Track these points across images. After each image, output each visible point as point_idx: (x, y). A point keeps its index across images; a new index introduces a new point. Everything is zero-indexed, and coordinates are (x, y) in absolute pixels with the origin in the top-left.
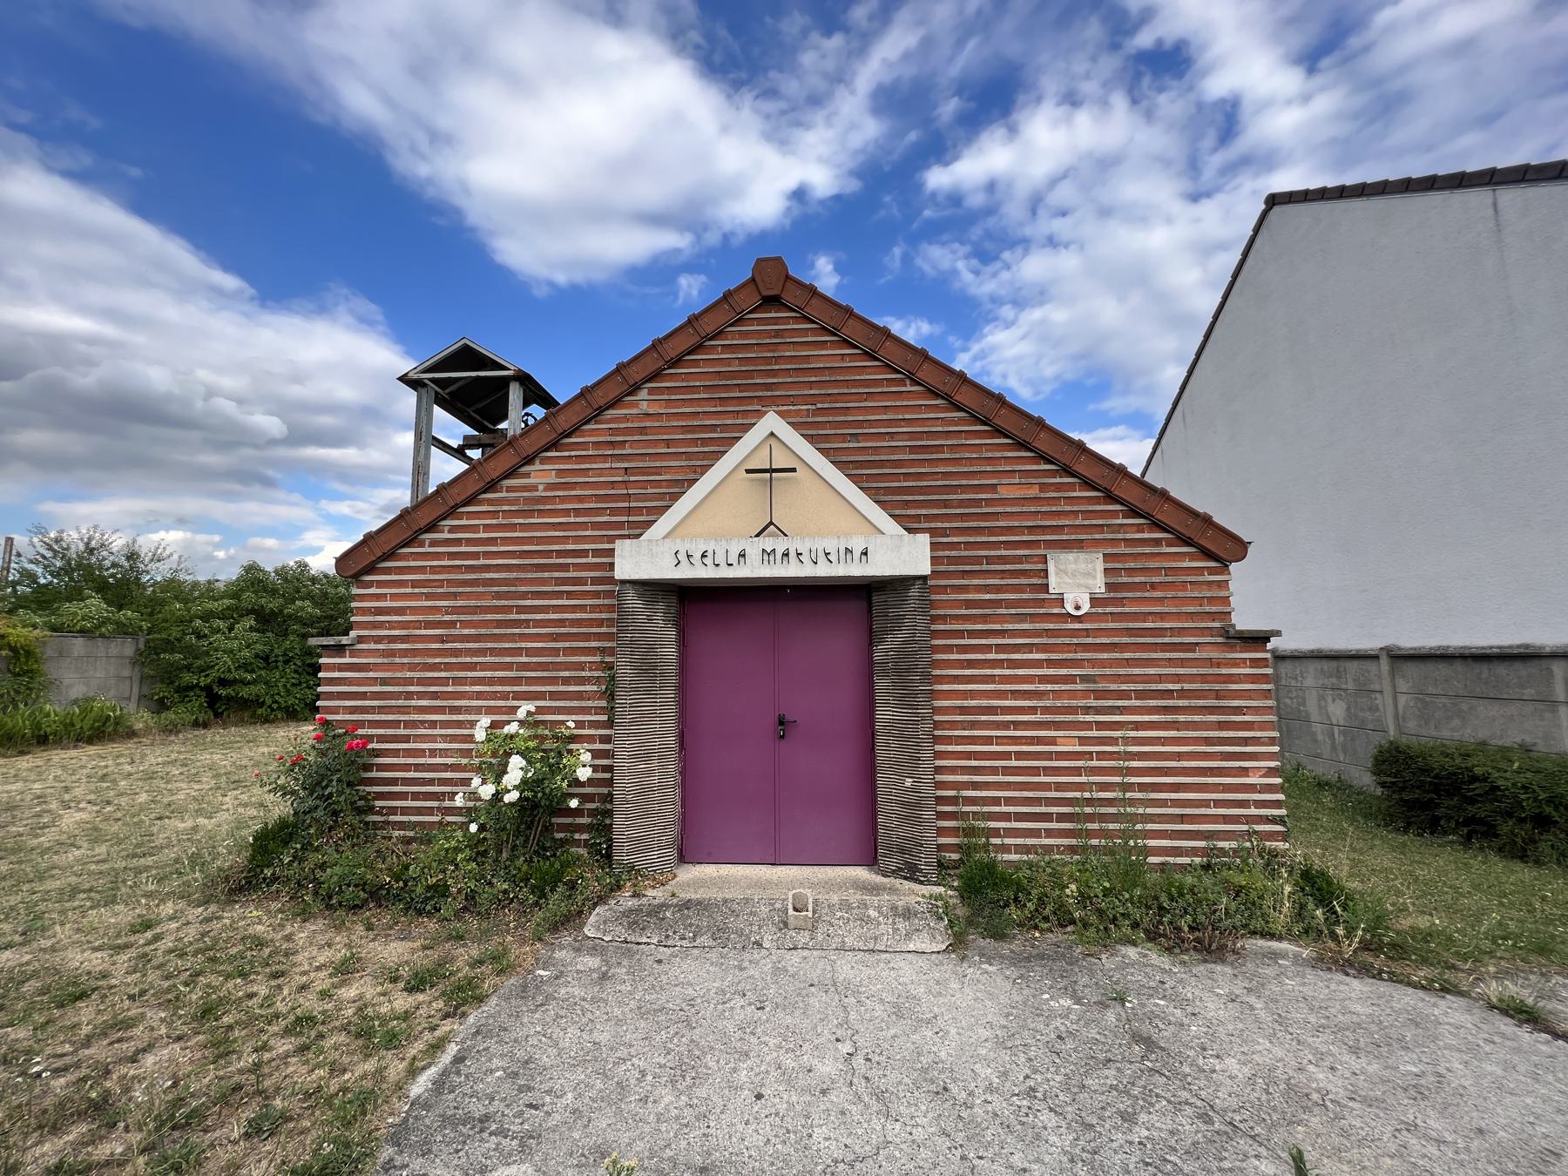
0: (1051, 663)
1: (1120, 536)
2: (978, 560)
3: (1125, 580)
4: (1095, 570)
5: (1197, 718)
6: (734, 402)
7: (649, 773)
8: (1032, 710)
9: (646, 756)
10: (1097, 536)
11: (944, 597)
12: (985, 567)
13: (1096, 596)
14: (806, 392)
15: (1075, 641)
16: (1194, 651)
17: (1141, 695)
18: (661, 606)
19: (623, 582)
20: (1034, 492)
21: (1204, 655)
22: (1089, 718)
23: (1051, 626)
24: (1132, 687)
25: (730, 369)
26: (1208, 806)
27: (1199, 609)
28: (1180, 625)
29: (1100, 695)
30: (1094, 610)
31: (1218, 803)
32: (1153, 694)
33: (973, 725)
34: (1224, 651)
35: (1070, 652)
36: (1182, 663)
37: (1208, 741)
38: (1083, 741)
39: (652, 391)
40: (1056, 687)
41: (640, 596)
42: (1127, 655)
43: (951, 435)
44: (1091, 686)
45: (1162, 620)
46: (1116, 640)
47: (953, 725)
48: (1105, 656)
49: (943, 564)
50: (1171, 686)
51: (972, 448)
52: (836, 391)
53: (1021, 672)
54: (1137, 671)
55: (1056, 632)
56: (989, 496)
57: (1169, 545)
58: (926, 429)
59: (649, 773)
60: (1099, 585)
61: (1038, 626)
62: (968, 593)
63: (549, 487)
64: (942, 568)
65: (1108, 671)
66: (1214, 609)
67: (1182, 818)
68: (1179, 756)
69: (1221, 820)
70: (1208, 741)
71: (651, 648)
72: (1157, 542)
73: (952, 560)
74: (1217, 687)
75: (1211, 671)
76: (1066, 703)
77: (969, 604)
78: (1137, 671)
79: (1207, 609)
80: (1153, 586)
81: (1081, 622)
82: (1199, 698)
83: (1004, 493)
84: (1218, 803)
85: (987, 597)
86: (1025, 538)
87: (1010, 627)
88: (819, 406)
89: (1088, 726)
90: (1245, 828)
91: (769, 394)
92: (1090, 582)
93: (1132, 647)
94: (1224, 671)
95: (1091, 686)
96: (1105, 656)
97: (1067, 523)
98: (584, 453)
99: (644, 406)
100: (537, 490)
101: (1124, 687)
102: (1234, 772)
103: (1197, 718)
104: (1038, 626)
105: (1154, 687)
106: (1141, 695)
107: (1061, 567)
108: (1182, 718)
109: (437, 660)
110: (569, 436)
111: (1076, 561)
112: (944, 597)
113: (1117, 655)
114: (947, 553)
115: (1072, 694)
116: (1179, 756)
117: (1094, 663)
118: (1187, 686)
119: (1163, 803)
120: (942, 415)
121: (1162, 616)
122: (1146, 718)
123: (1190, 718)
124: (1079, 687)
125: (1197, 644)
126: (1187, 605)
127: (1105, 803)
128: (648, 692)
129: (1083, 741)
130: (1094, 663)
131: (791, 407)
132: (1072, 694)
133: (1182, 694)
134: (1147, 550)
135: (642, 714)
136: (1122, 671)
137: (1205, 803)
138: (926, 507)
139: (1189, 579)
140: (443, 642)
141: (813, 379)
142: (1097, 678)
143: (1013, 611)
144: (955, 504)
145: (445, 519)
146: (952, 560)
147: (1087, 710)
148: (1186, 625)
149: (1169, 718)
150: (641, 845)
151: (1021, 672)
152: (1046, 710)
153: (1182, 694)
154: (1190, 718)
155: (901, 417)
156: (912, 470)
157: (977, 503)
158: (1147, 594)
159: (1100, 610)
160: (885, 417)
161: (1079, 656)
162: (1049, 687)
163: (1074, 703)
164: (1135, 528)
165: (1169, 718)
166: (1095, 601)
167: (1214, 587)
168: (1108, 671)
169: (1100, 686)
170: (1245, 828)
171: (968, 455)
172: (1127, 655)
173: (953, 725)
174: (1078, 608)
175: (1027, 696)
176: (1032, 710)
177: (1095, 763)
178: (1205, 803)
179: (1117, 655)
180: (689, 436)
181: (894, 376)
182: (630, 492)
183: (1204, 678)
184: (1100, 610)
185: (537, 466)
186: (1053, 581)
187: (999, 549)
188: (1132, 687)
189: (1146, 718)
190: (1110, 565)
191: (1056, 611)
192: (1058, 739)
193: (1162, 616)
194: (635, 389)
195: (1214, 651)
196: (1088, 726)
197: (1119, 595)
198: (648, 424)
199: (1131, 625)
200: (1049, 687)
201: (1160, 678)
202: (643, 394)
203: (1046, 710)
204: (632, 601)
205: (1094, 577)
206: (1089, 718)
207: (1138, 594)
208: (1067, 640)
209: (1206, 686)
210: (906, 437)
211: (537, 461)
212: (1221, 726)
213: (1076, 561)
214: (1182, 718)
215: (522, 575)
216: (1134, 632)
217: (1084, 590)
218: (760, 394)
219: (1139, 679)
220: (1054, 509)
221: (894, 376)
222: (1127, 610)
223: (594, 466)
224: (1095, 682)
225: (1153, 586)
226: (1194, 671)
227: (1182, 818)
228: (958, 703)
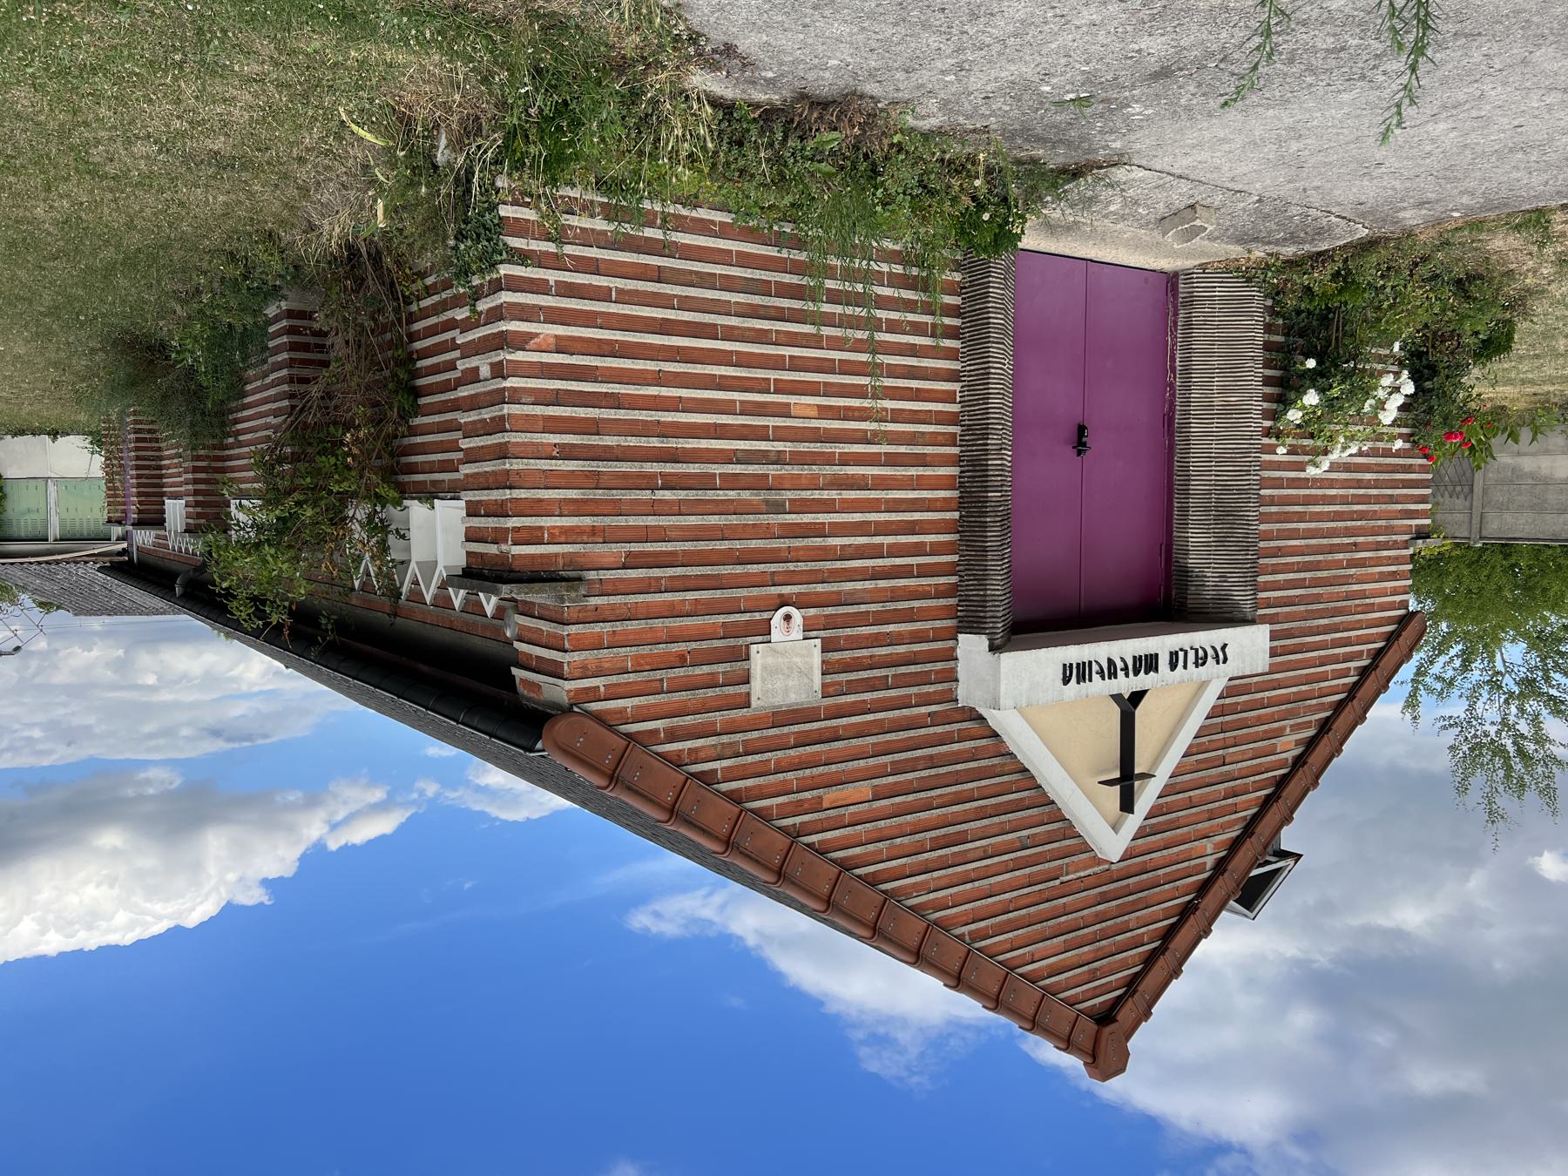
0: (818, 531)
1: (725, 739)
2: (901, 682)
3: (721, 668)
4: (763, 680)
5: (632, 442)
6: (1133, 870)
7: (1224, 391)
8: (846, 460)
9: (1228, 411)
10: (755, 734)
11: (938, 624)
12: (890, 672)
13: (760, 638)
14: (1070, 898)
15: (791, 566)
16: (629, 554)
17: (706, 482)
18: (1209, 594)
19: (1252, 622)
20: (830, 795)
21: (615, 548)
22: (780, 446)
23: (820, 588)
24: (721, 495)
25: (1138, 914)
26: (620, 291)
27: (619, 626)
28: (649, 598)
29: (759, 483)
30: (766, 615)
31: (603, 295)
32: (691, 482)
33: (912, 439)
34: (584, 555)
35: (797, 549)
36: (647, 535)
37: (615, 402)
38: (784, 411)
39: (1200, 869)
40: (817, 495)
41: (1236, 605)
42: (725, 545)
43: (923, 868)
44: (774, 496)
45: (672, 604)
46: (739, 569)
47: (933, 440)
48: (754, 544)
49: (937, 672)
50: (667, 495)
51: (901, 853)
52: (1042, 906)
53: (857, 517)
54: (714, 520)
55: (812, 578)
56: (884, 781)
57: (655, 732)
58: (950, 871)
59: (1224, 391)
60: (760, 657)
61: (834, 587)
62: (911, 632)
63: (1279, 733)
64: (939, 666)
65: (750, 519)
66: (597, 628)
67: (660, 276)
68: (659, 379)
69: (602, 267)
70: (615, 402)
71: (1221, 541)
72: (673, 736)
73: (922, 679)
74: (599, 494)
75: (608, 521)
76: (806, 471)
77: (908, 616)
78: (714, 520)
79: (607, 628)
80: (681, 661)
81: (781, 596)
82: (625, 475)
83: (864, 788)
84: (603, 295)
85: (891, 628)
86: (844, 721)
87: (869, 585)
88: (1057, 882)
89: (781, 435)
90: (569, 249)
91: (1104, 888)
92: (770, 660)
93: (714, 559)
94: (587, 521)
95: (774, 496)
96: (754, 544)
97: (792, 752)
98: (1257, 778)
99: (1208, 845)
100: (1291, 726)
101: (732, 494)
102: (578, 345)
103: (632, 442)
104: (834, 587)
105: (691, 495)
106: (706, 482)
107: (806, 680)
108: (655, 442)
109: (1359, 523)
110: (1268, 797)
111: (786, 691)
112: (938, 624)
113: (737, 545)
114: (931, 688)
115: (796, 484)
116: (659, 379)
117: (766, 532)
118: (646, 495)
119: (686, 304)
120: (932, 896)
121: (673, 612)
122: (704, 444)
123: (643, 442)
124: (790, 495)
125: (624, 567)
126: (635, 632)
127: (762, 312)
128: (1226, 489)
129: (784, 411)
130: (766, 532)
131: (1082, 874)
132: (796, 484)
133: (648, 482)
134: (689, 720)
135: (1232, 461)
136: (734, 520)
137: (625, 297)
138: (953, 753)
139: (632, 677)
140: (1355, 544)
141: (1063, 919)
142: (764, 508)
143: (863, 608)
144: (921, 764)
145: (1355, 684)
146: (922, 679)
147: (779, 459)
148: (640, 598)
149: (672, 443)
150: (1237, 306)
151: (857, 517)
152: (828, 460)
153: (648, 482)
154: (643, 442)
155: (977, 884)
156: (968, 806)
157: (898, 769)
158: (694, 645)
159: (757, 616)
160: (992, 880)
161: (788, 543)
162: (825, 495)
163: (796, 470)
164: (702, 755)
165: (672, 443)
166: (765, 630)
167: (592, 667)
168: (750, 519)
169: (763, 495)
170: (569, 249)
171: (905, 840)
172: (725, 545)
173: (933, 440)
174: (788, 618)
175: (850, 481)
176: (846, 460)
177: (772, 375)
178: (625, 297)
179: (737, 545)
180: (1174, 815)
181: (983, 943)
182: (1221, 736)
183: (617, 509)
184: (757, 616)
185: (1290, 755)
186: (812, 655)
187: (873, 701)
188: (721, 495)
189: (704, 444)
190: (743, 689)
191: (812, 612)
192: (815, 413)
193: (673, 612)
194: (1220, 866)
195: (600, 555)
196: (781, 435)
197: (732, 642)
198: (1207, 824)
199: (718, 594)
200: (825, 495)
201: (679, 509)
202: (1210, 861)
203: (828, 460)
204: (1242, 597)
205: (764, 668)
206: (780, 446)
207: (705, 645)
208: (802, 566)
209: (617, 494)
210: (971, 856)
211: (1290, 761)
212: (594, 427)
213: (786, 691)
214: (655, 442)
215: (1302, 624)
216: (714, 583)
217: (780, 647)
218: (1112, 886)
219: (710, 507)
220: (808, 771)
221: (983, 943)
222: (721, 619)
223: (1249, 763)
224: (767, 502)
225: (681, 661)
226: (633, 521)
227: (660, 276)
228: (929, 472)
